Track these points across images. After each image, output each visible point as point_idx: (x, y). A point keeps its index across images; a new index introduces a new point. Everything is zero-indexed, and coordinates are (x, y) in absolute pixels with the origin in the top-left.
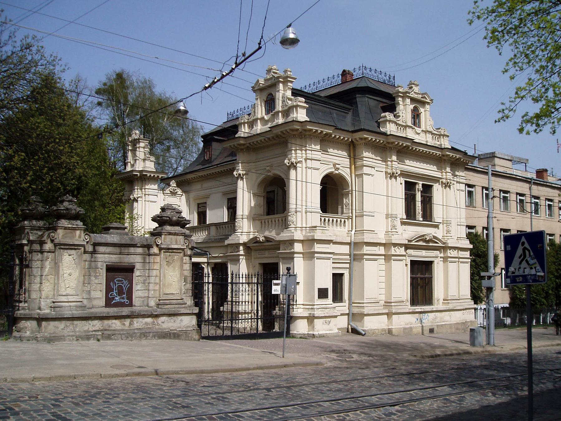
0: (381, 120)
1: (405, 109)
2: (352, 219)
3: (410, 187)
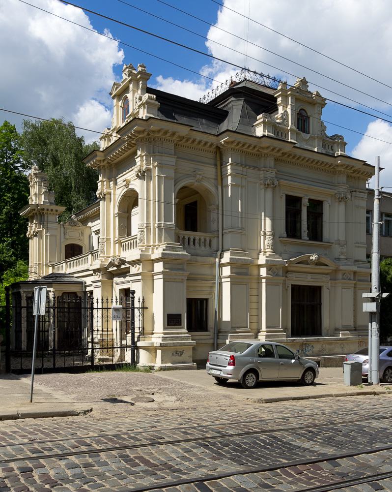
0: (257, 122)
1: (285, 111)
2: (218, 237)
3: (293, 203)
